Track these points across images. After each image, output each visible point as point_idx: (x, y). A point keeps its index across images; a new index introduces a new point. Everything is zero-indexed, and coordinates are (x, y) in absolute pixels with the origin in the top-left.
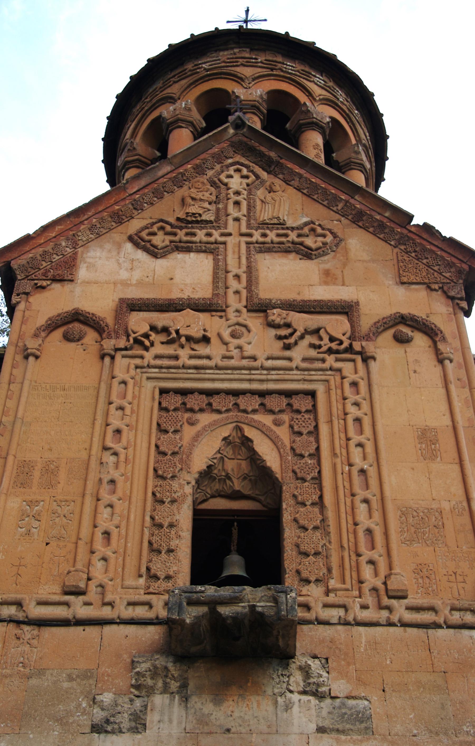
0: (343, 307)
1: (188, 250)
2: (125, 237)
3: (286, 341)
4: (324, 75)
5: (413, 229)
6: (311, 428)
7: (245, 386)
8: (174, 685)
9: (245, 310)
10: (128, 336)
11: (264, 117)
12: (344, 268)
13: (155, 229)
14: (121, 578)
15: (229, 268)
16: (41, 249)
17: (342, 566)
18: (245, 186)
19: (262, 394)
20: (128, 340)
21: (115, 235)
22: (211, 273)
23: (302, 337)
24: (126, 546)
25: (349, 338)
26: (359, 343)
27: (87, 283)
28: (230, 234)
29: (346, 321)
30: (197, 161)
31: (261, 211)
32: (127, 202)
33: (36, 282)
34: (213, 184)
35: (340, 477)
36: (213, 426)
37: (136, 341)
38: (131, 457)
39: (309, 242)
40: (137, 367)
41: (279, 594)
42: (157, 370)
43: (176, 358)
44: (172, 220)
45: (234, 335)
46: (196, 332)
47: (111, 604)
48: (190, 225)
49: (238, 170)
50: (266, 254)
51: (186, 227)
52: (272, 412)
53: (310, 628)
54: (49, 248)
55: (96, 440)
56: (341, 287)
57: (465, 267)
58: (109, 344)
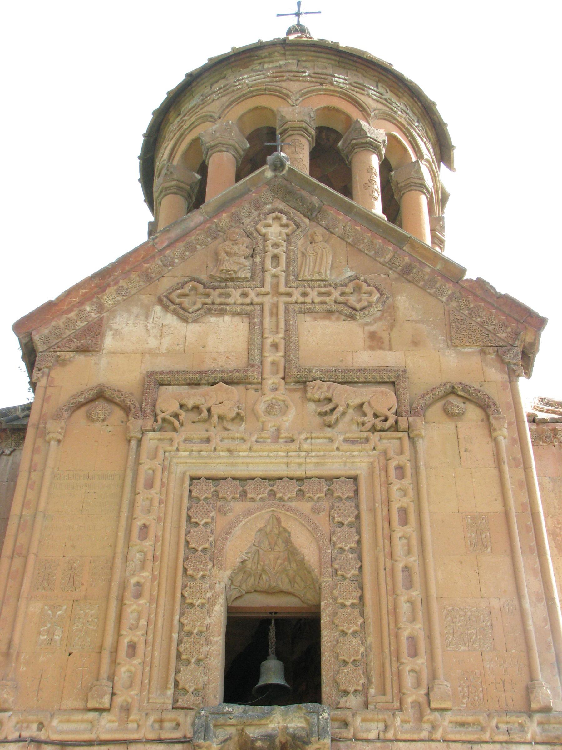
1: (222, 313)
2: (154, 299)
3: (327, 418)
4: (380, 85)
5: (466, 285)
10: (156, 416)
11: (312, 138)
12: (391, 330)
13: (186, 290)
14: (147, 691)
17: (382, 674)
18: (285, 237)
20: (156, 421)
21: (144, 296)
22: (246, 339)
23: (344, 414)
24: (152, 655)
25: (396, 413)
26: (406, 418)
29: (393, 394)
31: (302, 264)
33: (58, 354)
35: (382, 573)
38: (158, 553)
39: (352, 300)
41: (311, 715)
42: (187, 453)
44: (204, 277)
48: (224, 284)
49: (277, 218)
53: (347, 746)
54: (72, 315)
55: (121, 534)
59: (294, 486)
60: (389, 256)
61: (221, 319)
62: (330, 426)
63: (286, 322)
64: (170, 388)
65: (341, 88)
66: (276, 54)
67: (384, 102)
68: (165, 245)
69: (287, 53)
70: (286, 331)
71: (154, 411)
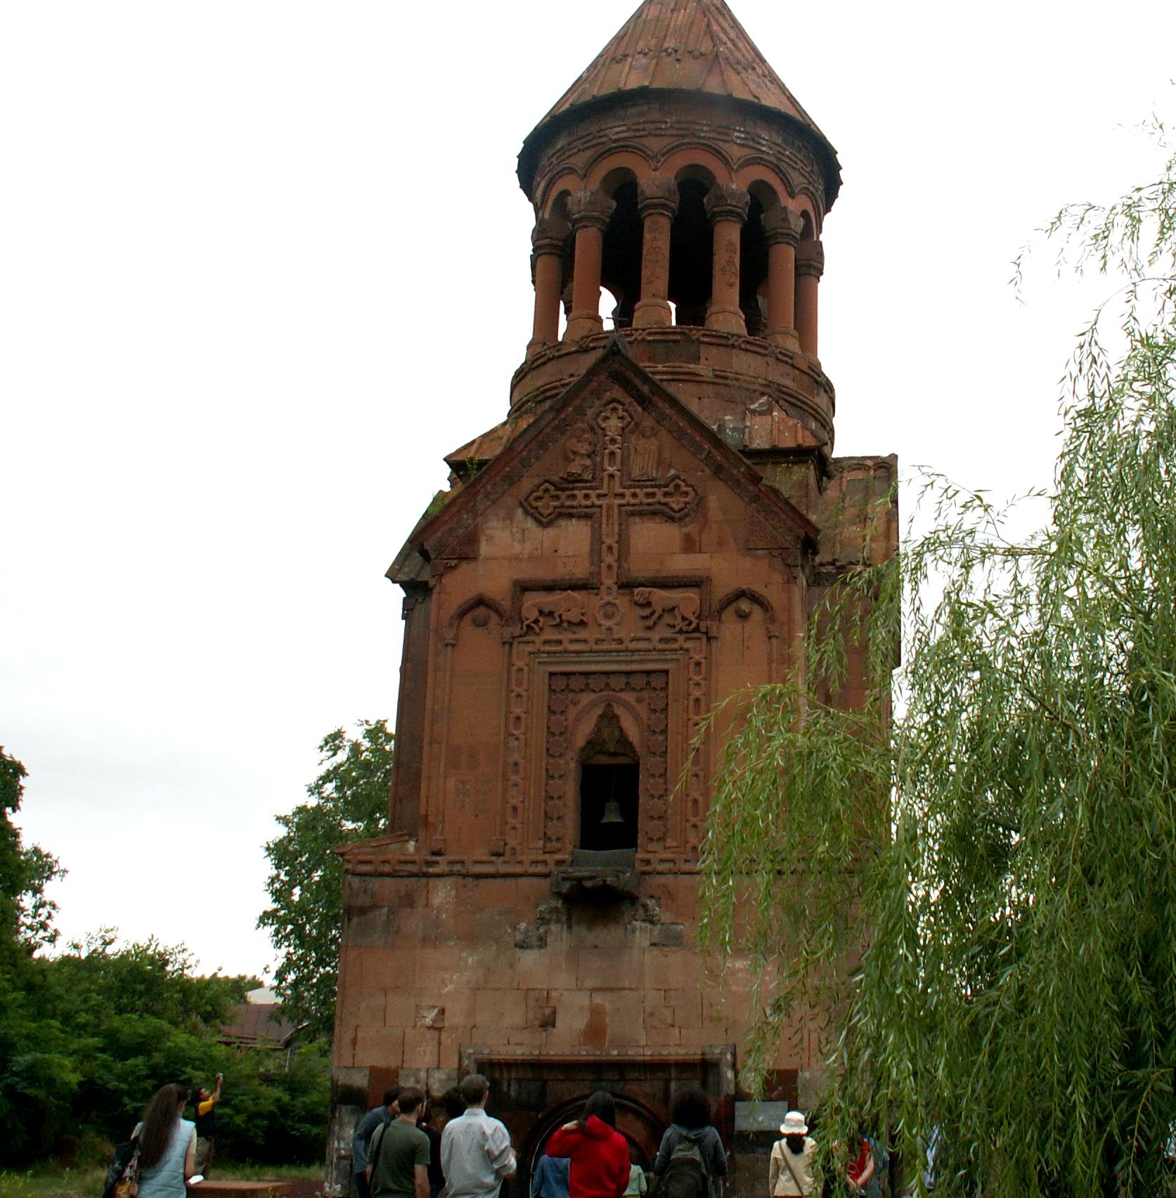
1: (571, 516)
6: (663, 706)
7: (614, 667)
8: (564, 918)
11: (673, 213)
13: (540, 493)
15: (604, 538)
19: (628, 673)
23: (661, 616)
30: (578, 402)
32: (516, 461)
34: (592, 429)
36: (593, 704)
37: (528, 626)
40: (530, 653)
43: (559, 642)
45: (607, 617)
46: (574, 616)
47: (520, 862)
48: (570, 486)
49: (615, 409)
51: (567, 489)
52: (634, 689)
57: (803, 536)
58: (508, 632)
59: (623, 679)
62: (649, 628)
71: (520, 618)
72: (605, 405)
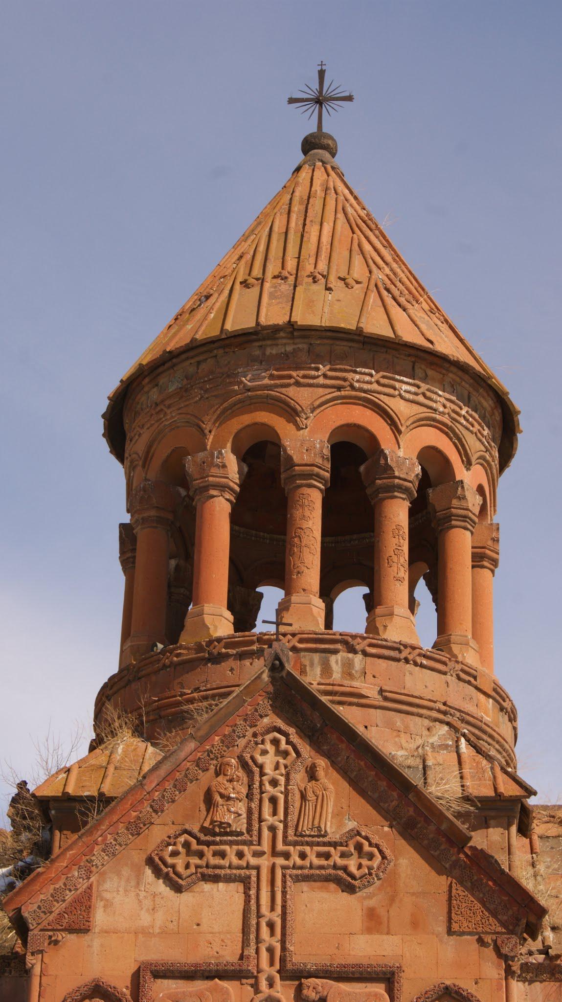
0: (385, 973)
1: (216, 879)
2: (145, 857)
9: (278, 975)
12: (391, 905)
16: (52, 887)
27: (106, 932)
28: (263, 853)
29: (387, 997)
33: (51, 933)
39: (352, 864)
48: (218, 839)
49: (275, 742)
50: (303, 883)
51: (214, 843)
54: (61, 884)
56: (385, 937)
60: (395, 803)
61: (214, 886)
63: (284, 893)
64: (166, 982)
65: (365, 391)
66: (282, 334)
67: (421, 399)
68: (154, 785)
69: (295, 334)
70: (284, 907)
72: (263, 734)
